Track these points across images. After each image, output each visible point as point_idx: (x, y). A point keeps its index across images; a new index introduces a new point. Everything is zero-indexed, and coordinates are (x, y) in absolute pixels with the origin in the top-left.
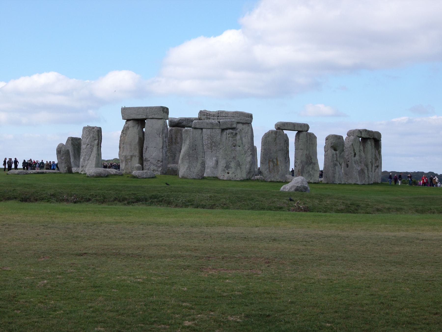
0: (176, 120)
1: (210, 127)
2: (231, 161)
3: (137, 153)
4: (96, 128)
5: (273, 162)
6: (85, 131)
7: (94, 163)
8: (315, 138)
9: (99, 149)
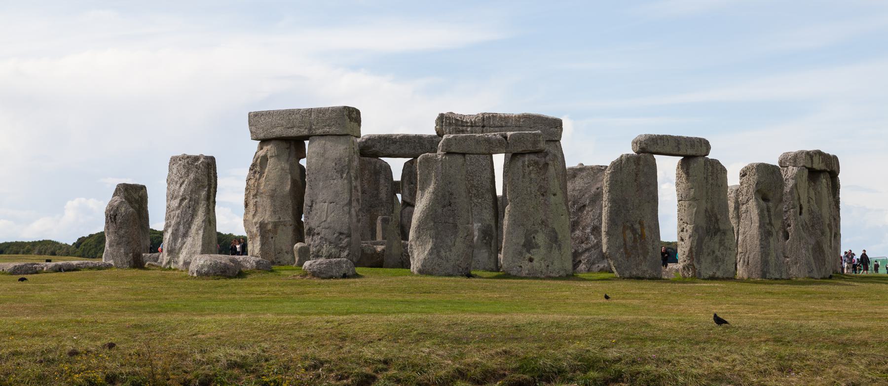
1: (483, 151)
2: (536, 232)
3: (288, 218)
4: (202, 159)
5: (634, 231)
6: (175, 166)
7: (200, 243)
8: (724, 171)
9: (211, 207)
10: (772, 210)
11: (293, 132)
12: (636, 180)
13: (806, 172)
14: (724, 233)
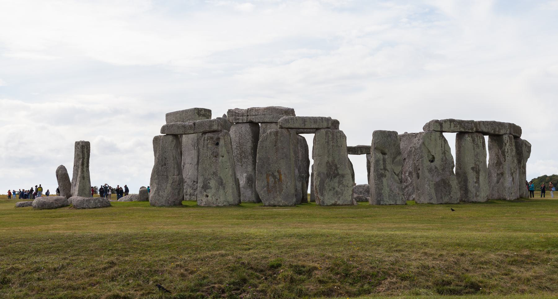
2: (210, 179)
5: (274, 177)
9: (85, 169)
10: (388, 161)
12: (275, 146)
14: (343, 176)
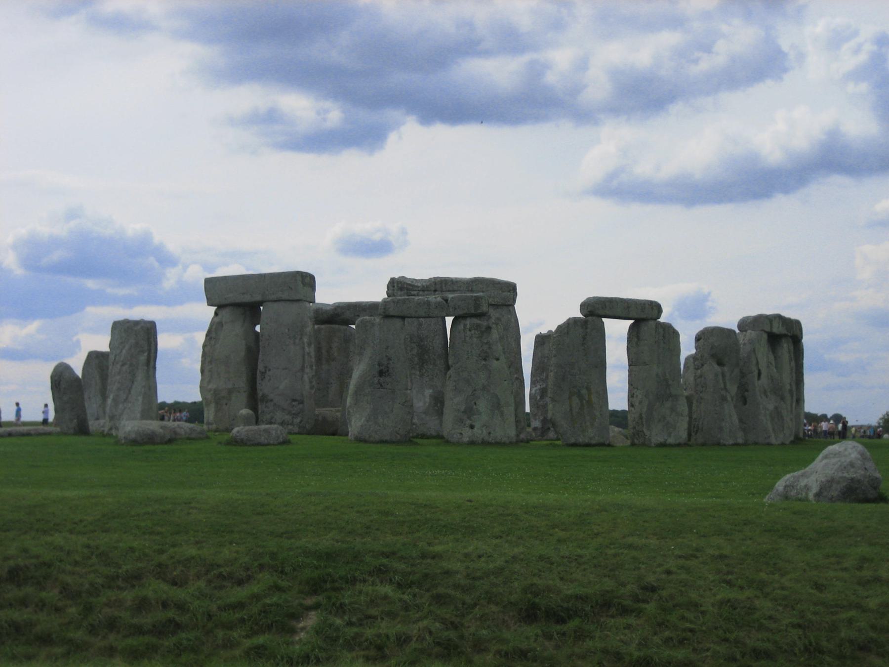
0: (328, 308)
3: (242, 383)
8: (676, 334)
11: (247, 299)
12: (583, 344)
13: (765, 336)
